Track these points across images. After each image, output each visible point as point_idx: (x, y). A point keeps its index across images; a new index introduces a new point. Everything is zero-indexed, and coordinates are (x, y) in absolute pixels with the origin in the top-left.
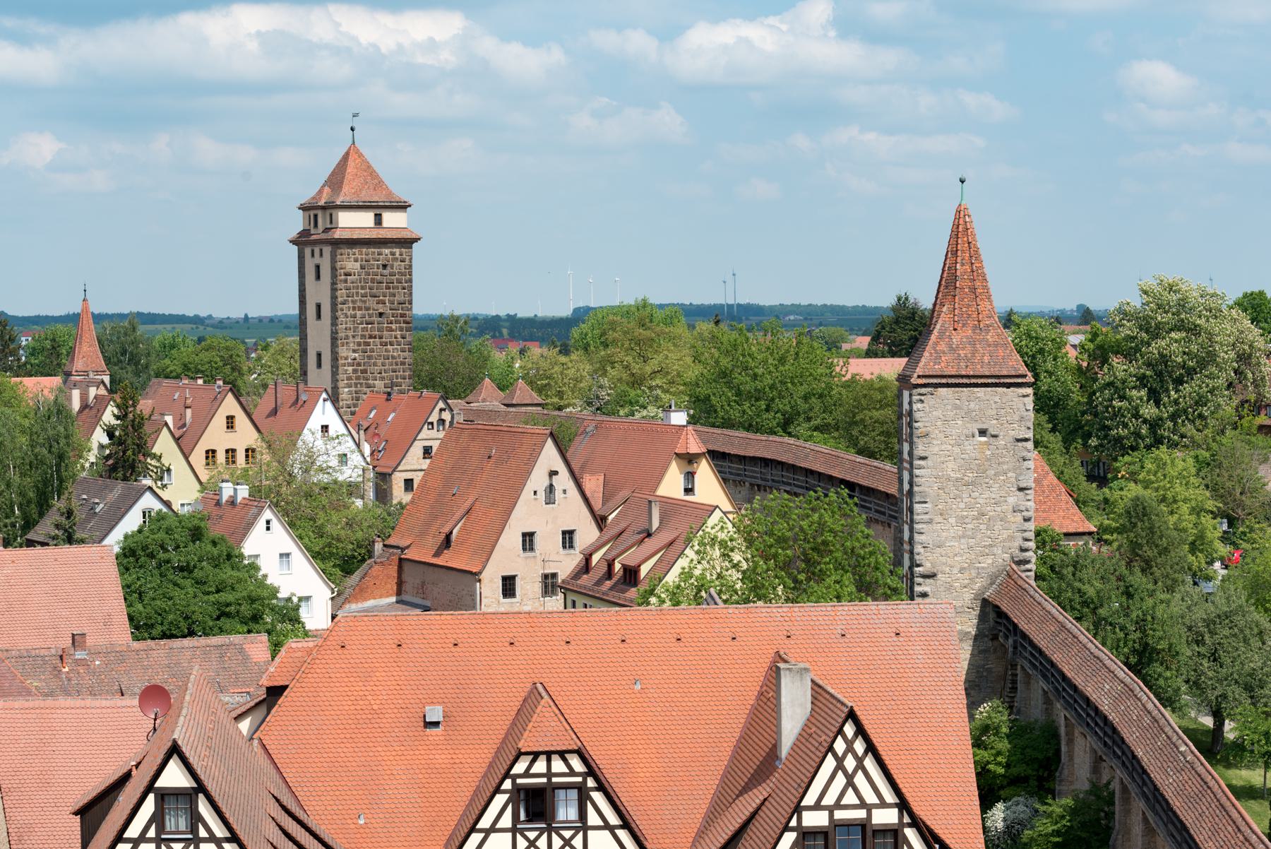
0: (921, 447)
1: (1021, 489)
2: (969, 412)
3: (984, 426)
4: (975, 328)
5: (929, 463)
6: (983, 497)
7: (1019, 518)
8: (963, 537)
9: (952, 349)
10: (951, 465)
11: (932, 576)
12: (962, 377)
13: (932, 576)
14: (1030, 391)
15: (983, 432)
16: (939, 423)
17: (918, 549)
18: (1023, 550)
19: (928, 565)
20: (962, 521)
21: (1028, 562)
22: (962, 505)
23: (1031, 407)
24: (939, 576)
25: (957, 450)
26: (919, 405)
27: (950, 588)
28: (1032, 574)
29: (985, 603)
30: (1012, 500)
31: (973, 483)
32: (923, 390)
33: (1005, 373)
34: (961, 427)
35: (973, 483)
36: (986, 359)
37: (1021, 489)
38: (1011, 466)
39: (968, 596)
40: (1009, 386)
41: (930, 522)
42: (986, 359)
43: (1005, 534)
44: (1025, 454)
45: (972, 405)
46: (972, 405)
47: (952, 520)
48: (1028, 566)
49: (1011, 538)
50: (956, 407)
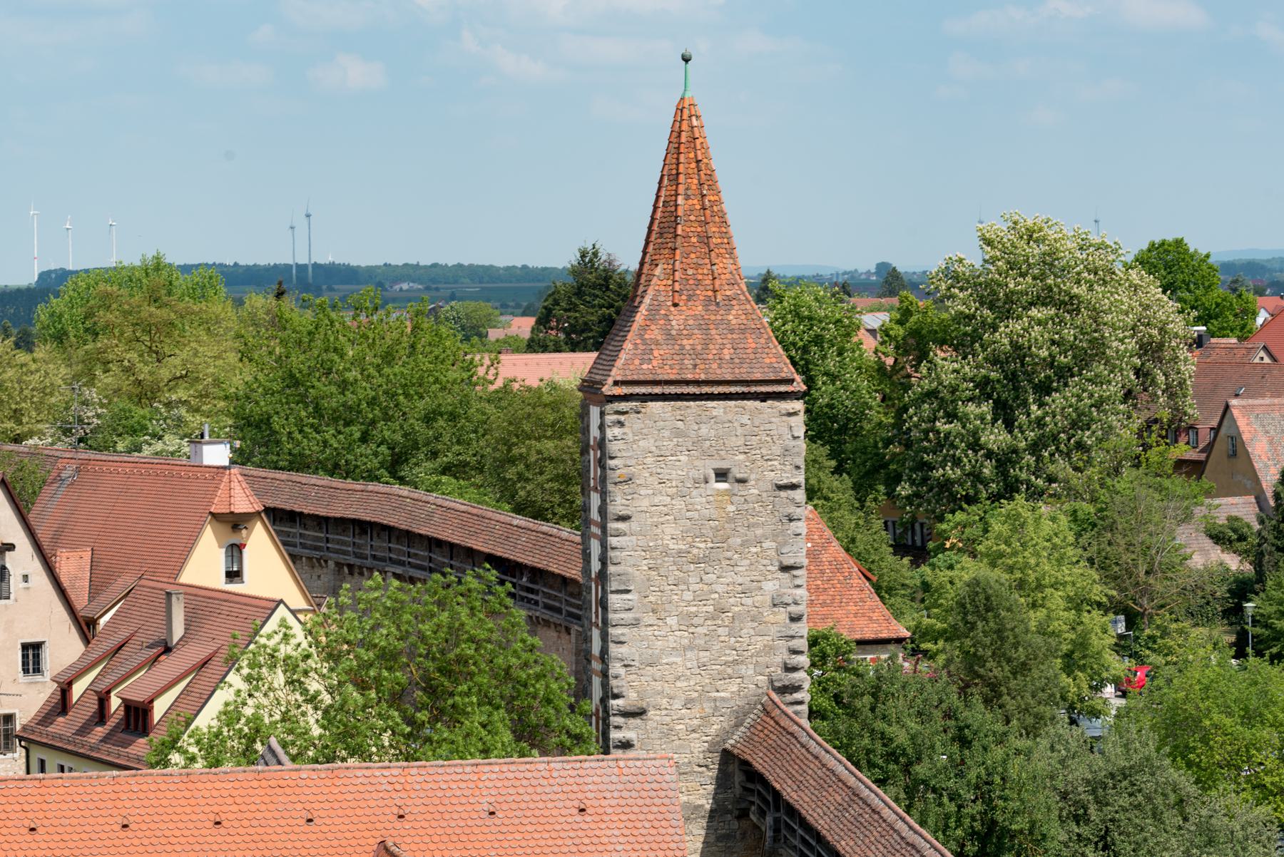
0: (619, 500)
1: (785, 569)
2: (699, 441)
3: (724, 465)
4: (708, 302)
5: (633, 525)
6: (722, 582)
7: (782, 615)
8: (690, 647)
9: (669, 336)
10: (669, 530)
11: (639, 713)
12: (688, 383)
13: (639, 713)
14: (799, 405)
15: (722, 475)
16: (649, 460)
17: (616, 668)
18: (790, 669)
19: (632, 695)
20: (688, 621)
21: (797, 688)
22: (688, 596)
23: (801, 431)
24: (651, 713)
25: (679, 504)
26: (617, 431)
27: (668, 733)
28: (805, 708)
29: (727, 757)
30: (770, 587)
31: (705, 560)
32: (623, 406)
33: (758, 376)
34: (684, 466)
35: (705, 560)
36: (727, 354)
37: (785, 569)
38: (768, 529)
39: (698, 747)
40: (764, 397)
41: (635, 624)
42: (727, 354)
43: (760, 643)
44: (791, 509)
45: (704, 430)
46: (704, 430)
47: (672, 621)
48: (798, 696)
49: (769, 649)
50: (678, 433)
